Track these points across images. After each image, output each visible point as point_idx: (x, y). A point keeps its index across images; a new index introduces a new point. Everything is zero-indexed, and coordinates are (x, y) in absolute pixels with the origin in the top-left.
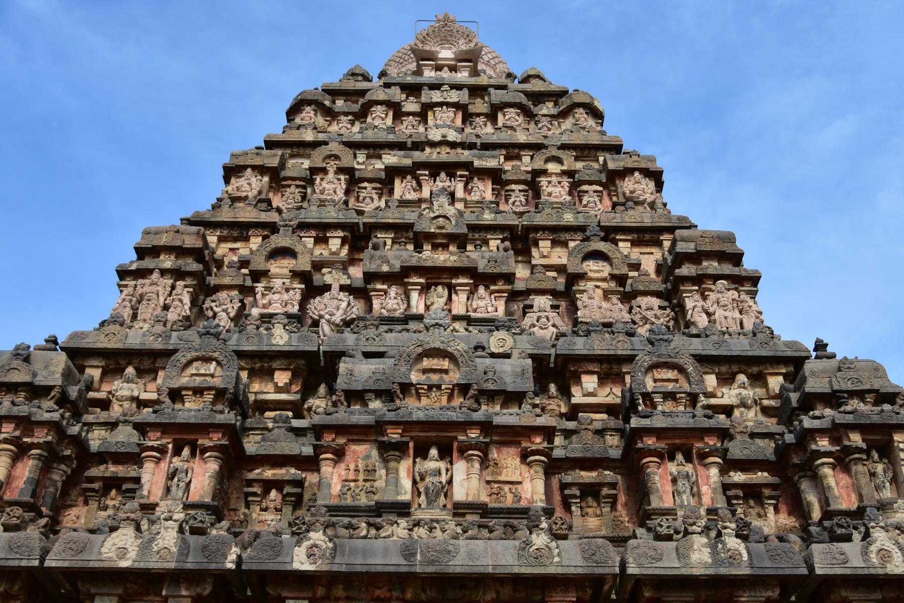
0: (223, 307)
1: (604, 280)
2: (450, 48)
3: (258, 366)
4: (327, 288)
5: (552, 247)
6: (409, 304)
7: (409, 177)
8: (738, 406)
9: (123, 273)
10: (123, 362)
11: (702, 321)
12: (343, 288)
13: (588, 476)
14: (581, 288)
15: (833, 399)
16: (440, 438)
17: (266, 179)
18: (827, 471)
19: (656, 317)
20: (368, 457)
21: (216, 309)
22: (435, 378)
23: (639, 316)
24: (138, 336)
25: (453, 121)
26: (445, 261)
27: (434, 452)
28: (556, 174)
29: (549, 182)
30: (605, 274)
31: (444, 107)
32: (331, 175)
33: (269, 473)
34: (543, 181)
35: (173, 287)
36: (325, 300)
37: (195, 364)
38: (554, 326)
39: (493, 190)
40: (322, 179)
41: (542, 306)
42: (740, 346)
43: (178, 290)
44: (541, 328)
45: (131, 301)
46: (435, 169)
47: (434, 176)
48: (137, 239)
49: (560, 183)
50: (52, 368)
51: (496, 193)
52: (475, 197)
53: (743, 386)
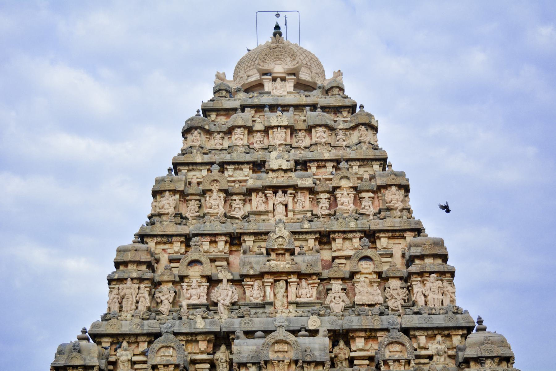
0: (166, 293)
1: (370, 273)
2: (281, 64)
3: (190, 338)
4: (220, 281)
5: (344, 242)
6: (265, 292)
7: (260, 193)
8: (436, 355)
9: (110, 281)
10: (121, 339)
11: (421, 301)
12: (228, 281)
14: (357, 280)
17: (177, 196)
19: (398, 295)
21: (163, 298)
22: (281, 356)
23: (389, 294)
24: (127, 325)
25: (285, 140)
26: (283, 268)
28: (346, 188)
29: (342, 194)
30: (371, 270)
31: (279, 128)
32: (215, 194)
34: (338, 193)
35: (139, 288)
36: (220, 290)
37: (163, 350)
38: (343, 301)
39: (310, 198)
40: (210, 197)
41: (337, 290)
42: (439, 321)
43: (142, 290)
44: (336, 304)
45: (118, 298)
46: (275, 189)
47: (275, 193)
48: (113, 256)
49: (348, 194)
50: (92, 355)
51: (312, 200)
52: (299, 207)
53: (439, 343)
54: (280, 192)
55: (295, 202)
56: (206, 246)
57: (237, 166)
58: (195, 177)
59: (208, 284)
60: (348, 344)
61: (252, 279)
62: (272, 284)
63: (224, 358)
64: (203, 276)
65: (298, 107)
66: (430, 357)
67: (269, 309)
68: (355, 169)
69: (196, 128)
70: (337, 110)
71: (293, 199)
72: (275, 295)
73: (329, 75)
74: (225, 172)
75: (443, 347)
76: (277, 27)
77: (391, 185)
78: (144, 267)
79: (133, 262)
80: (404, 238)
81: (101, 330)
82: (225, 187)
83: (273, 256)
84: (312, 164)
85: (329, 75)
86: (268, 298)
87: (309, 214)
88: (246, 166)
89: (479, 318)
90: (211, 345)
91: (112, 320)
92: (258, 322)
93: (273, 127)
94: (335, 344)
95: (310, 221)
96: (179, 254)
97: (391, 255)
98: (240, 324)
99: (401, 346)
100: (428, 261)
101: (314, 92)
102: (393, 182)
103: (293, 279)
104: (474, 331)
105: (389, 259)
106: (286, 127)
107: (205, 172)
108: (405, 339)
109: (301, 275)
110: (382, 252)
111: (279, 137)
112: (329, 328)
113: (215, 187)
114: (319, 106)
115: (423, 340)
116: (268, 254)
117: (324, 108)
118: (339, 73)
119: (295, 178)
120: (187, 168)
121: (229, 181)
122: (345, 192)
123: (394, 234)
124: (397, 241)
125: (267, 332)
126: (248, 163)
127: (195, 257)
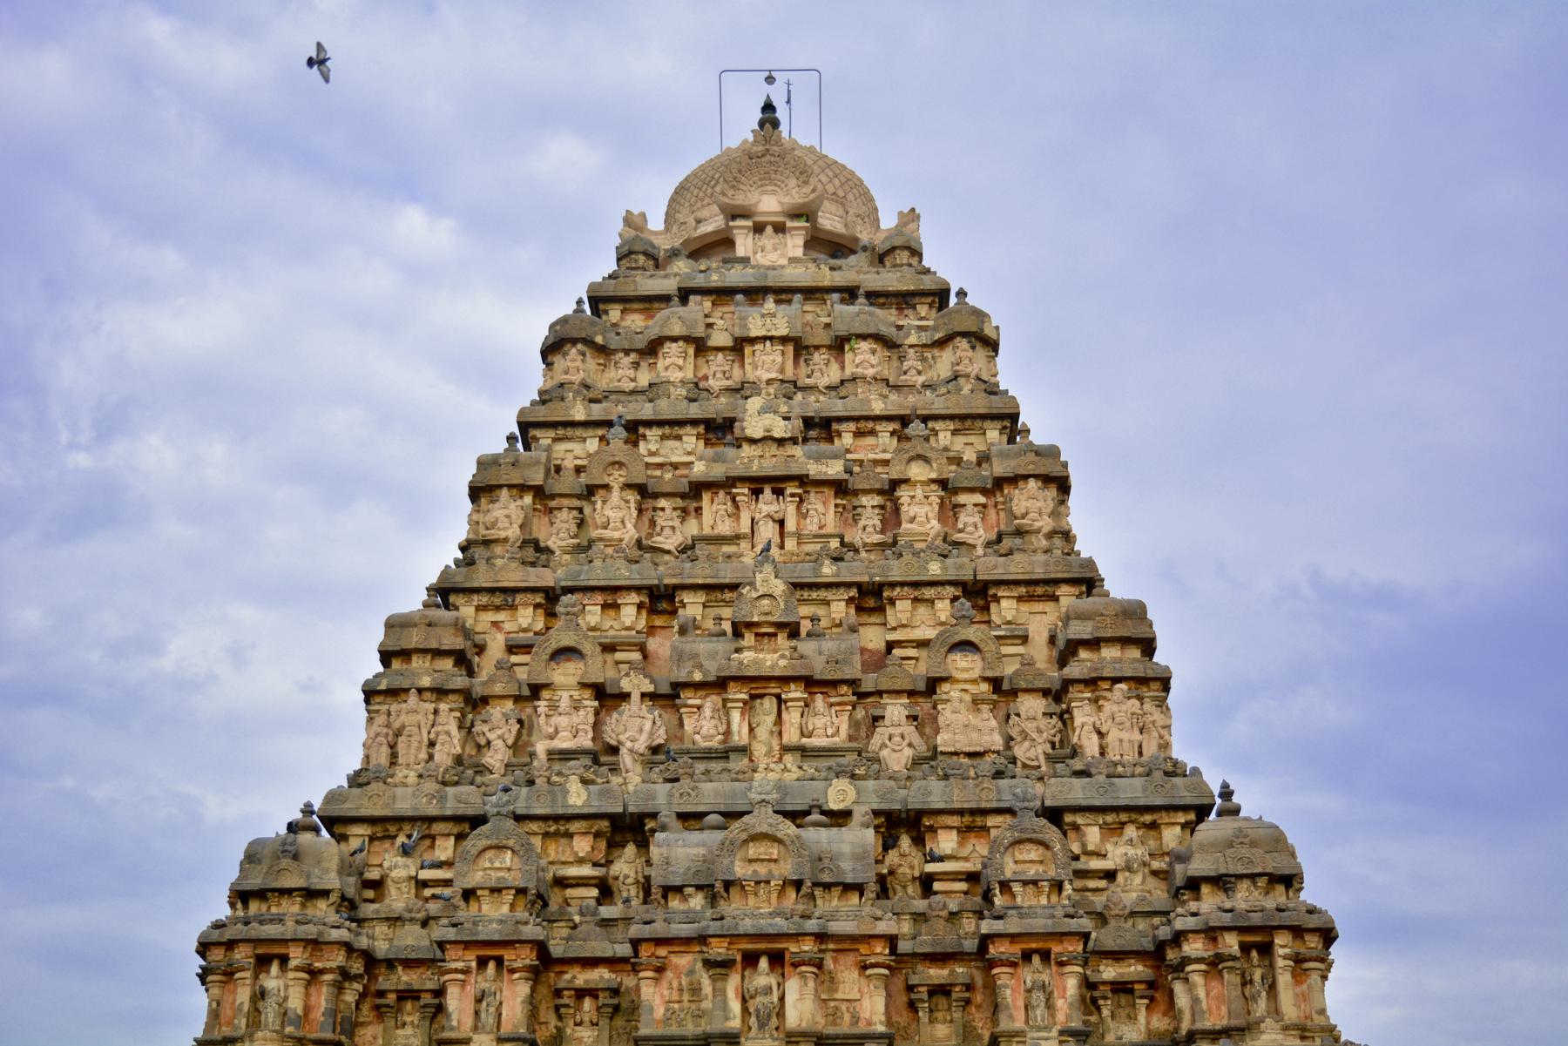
0: (498, 726)
1: (974, 681)
2: (774, 193)
3: (552, 829)
4: (625, 697)
5: (914, 608)
7: (722, 493)
9: (370, 693)
10: (392, 829)
11: (1091, 745)
12: (643, 695)
13: (937, 974)
15: (1222, 882)
16: (769, 951)
18: (1197, 979)
19: (1039, 731)
20: (691, 972)
21: (491, 736)
22: (762, 870)
23: (1017, 729)
24: (408, 794)
25: (782, 371)
26: (772, 667)
27: (764, 963)
28: (923, 483)
29: (913, 497)
30: (976, 674)
32: (616, 495)
33: (582, 977)
34: (903, 493)
35: (436, 712)
37: (489, 854)
38: (910, 745)
40: (604, 502)
42: (1131, 791)
43: (442, 718)
45: (387, 735)
46: (757, 484)
47: (757, 492)
49: (927, 497)
50: (326, 865)
51: (841, 511)
52: (811, 526)
53: (1130, 842)
54: (767, 490)
55: (802, 516)
56: (593, 614)
57: (667, 430)
58: (570, 456)
59: (596, 703)
60: (919, 841)
61: (700, 693)
62: (745, 703)
63: (632, 874)
65: (812, 293)
66: (1110, 875)
67: (738, 763)
68: (944, 438)
69: (574, 341)
70: (903, 300)
71: (798, 508)
72: (751, 730)
73: (888, 221)
74: (642, 444)
75: (1139, 852)
76: (768, 107)
77: (1026, 477)
79: (423, 651)
80: (1055, 598)
81: (348, 809)
82: (640, 480)
83: (749, 639)
84: (843, 427)
85: (888, 221)
88: (689, 429)
89: (1225, 786)
90: (603, 845)
91: (373, 785)
92: (711, 792)
94: (889, 844)
95: (836, 559)
96: (531, 634)
97: (1025, 639)
98: (670, 795)
99: (1041, 849)
100: (1110, 653)
101: (852, 259)
102: (1031, 469)
103: (795, 692)
104: (1213, 815)
105: (1020, 649)
106: (784, 340)
107: (593, 445)
108: (1051, 833)
109: (811, 683)
110: (1002, 633)
111: (767, 364)
112: (876, 807)
113: (616, 479)
114: (861, 291)
115: (1093, 835)
116: (737, 634)
117: (874, 297)
118: (912, 216)
119: (802, 459)
120: (551, 433)
121: (648, 465)
122: (919, 492)
123: (1031, 589)
124: (1038, 607)
125: (732, 815)
126: (694, 422)
127: (568, 640)
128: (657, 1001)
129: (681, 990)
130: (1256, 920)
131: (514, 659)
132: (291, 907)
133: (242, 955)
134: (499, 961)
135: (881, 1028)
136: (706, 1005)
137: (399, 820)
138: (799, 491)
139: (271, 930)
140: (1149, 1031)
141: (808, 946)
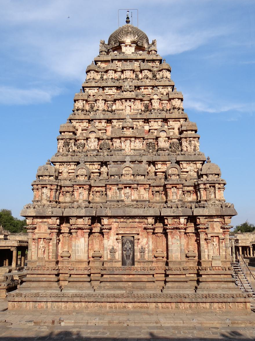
10: (63, 164)
11: (185, 149)
22: (127, 172)
30: (165, 136)
32: (100, 101)
34: (152, 101)
40: (98, 103)
46: (126, 99)
47: (126, 101)
52: (136, 107)
54: (128, 100)
57: (110, 88)
58: (92, 93)
59: (98, 141)
60: (154, 166)
61: (116, 139)
62: (124, 141)
63: (105, 171)
64: (95, 138)
66: (187, 172)
67: (123, 152)
69: (92, 70)
70: (153, 61)
74: (105, 90)
75: (193, 168)
76: (128, 18)
77: (175, 98)
78: (72, 133)
82: (105, 98)
86: (123, 147)
87: (140, 111)
90: (100, 166)
91: (60, 156)
93: (125, 70)
95: (140, 114)
96: (86, 127)
97: (174, 129)
100: (189, 132)
102: (176, 97)
103: (133, 139)
105: (173, 131)
106: (131, 70)
107: (96, 91)
108: (177, 166)
109: (136, 138)
110: (170, 128)
111: (128, 74)
113: (101, 98)
114: (145, 60)
117: (148, 61)
120: (88, 88)
121: (106, 95)
122: (156, 101)
123: (175, 120)
128: (110, 194)
129: (114, 193)
130: (212, 182)
131: (83, 132)
132: (47, 178)
133: (40, 186)
134: (83, 187)
135: (148, 199)
136: (118, 195)
137: (65, 162)
138: (134, 101)
139: (44, 183)
140: (193, 199)
141: (136, 186)
